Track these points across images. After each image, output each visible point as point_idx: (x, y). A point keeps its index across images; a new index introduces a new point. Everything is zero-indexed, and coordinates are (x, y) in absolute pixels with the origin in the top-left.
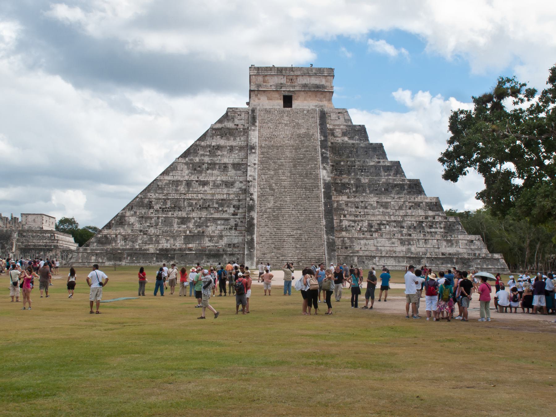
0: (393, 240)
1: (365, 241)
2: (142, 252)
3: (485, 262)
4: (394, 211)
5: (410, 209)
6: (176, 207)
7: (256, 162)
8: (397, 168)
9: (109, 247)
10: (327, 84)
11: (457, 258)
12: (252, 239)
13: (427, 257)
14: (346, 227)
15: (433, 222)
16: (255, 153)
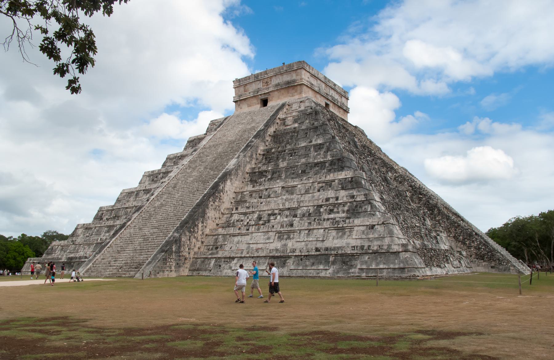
0: (270, 233)
1: (239, 237)
3: (376, 259)
4: (300, 196)
5: (319, 191)
8: (330, 144)
10: (298, 77)
11: (336, 255)
13: (296, 256)
14: (233, 223)
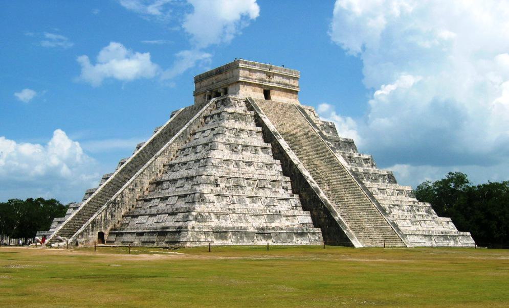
2: (243, 231)
6: (237, 186)
7: (289, 148)
9: (207, 224)
11: (450, 236)
12: (339, 219)
15: (418, 207)
16: (280, 138)
